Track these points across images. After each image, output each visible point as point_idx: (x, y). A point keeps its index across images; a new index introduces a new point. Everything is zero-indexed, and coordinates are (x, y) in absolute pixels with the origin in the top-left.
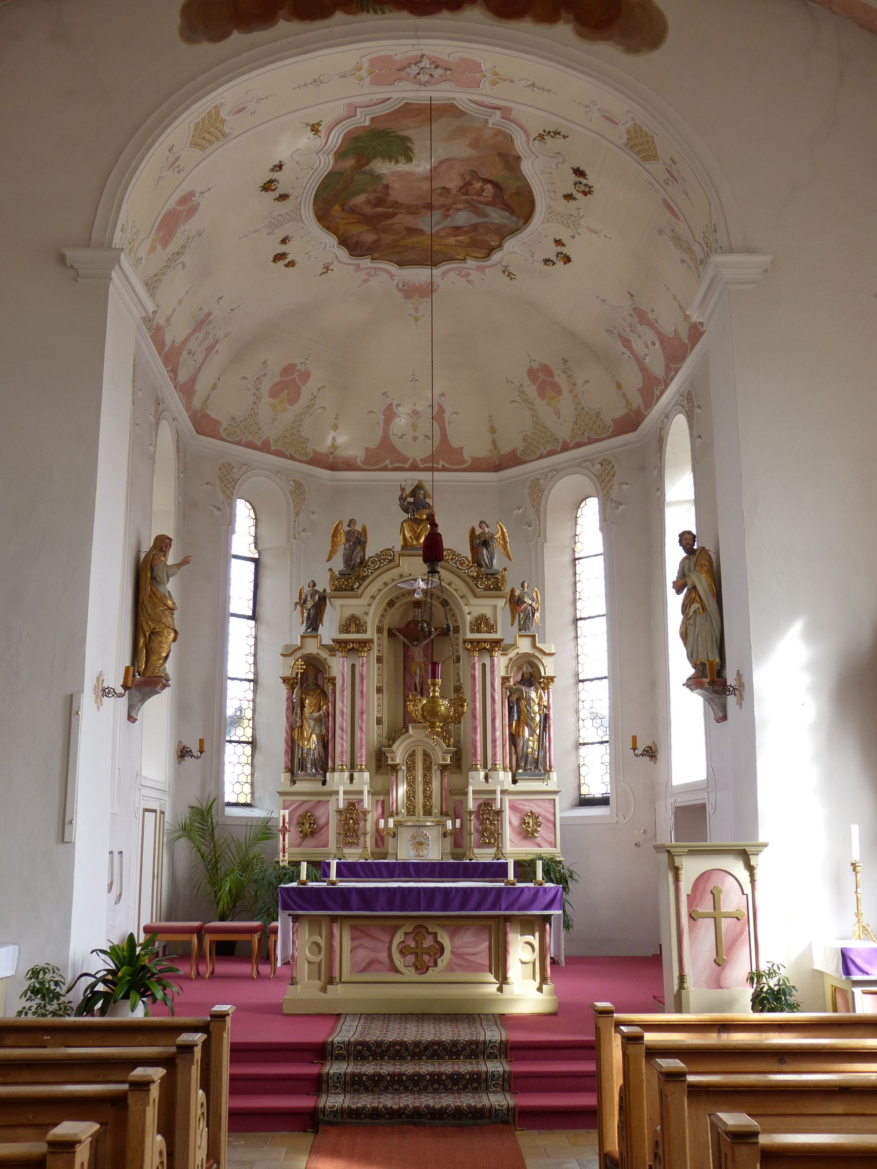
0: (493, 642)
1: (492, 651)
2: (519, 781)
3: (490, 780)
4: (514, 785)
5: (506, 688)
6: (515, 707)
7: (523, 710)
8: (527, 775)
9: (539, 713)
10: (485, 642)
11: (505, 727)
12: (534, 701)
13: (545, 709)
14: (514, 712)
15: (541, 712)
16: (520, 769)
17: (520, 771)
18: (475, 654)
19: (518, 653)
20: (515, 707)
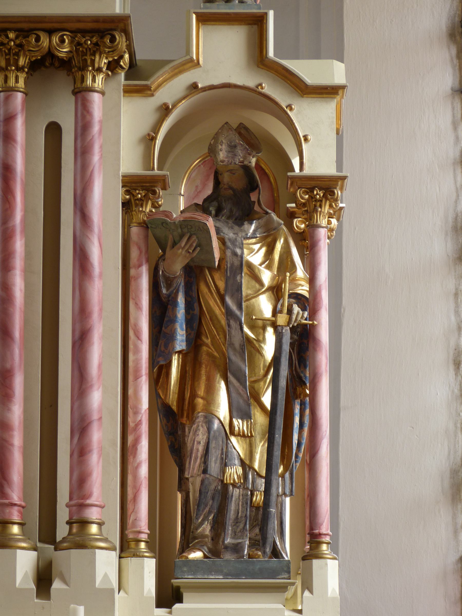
0: (84, 32)
1: (83, 68)
2: (186, 596)
3: (57, 585)
4: (162, 611)
5: (145, 225)
6: (181, 300)
7: (211, 311)
8: (218, 572)
9: (274, 325)
10: (50, 32)
11: (137, 377)
12: (257, 279)
13: (296, 309)
14: (173, 320)
15: (282, 319)
16: (194, 549)
17: (197, 555)
18: (12, 82)
19: (194, 86)
20: (181, 300)
